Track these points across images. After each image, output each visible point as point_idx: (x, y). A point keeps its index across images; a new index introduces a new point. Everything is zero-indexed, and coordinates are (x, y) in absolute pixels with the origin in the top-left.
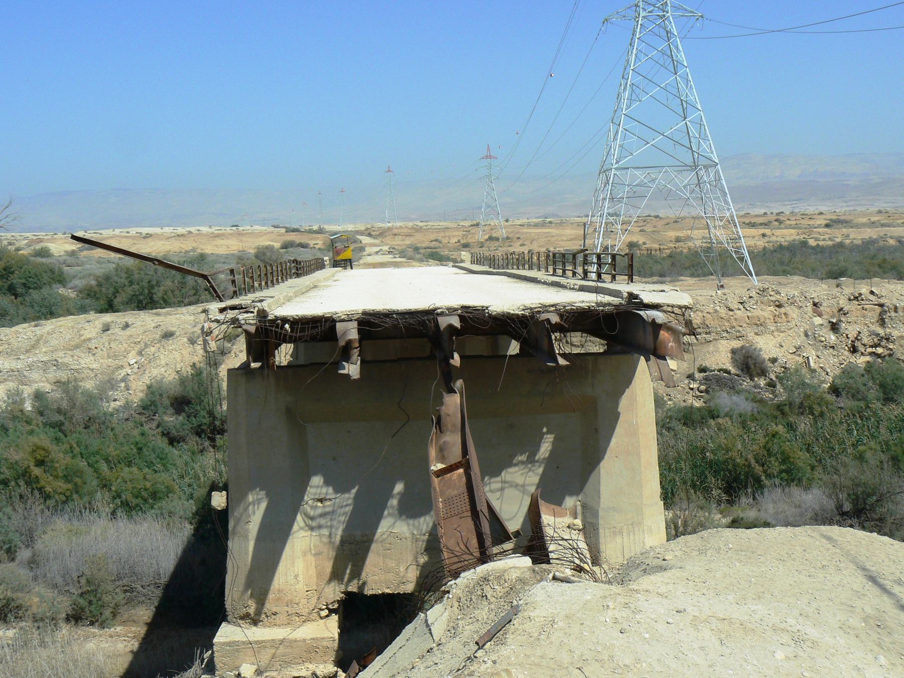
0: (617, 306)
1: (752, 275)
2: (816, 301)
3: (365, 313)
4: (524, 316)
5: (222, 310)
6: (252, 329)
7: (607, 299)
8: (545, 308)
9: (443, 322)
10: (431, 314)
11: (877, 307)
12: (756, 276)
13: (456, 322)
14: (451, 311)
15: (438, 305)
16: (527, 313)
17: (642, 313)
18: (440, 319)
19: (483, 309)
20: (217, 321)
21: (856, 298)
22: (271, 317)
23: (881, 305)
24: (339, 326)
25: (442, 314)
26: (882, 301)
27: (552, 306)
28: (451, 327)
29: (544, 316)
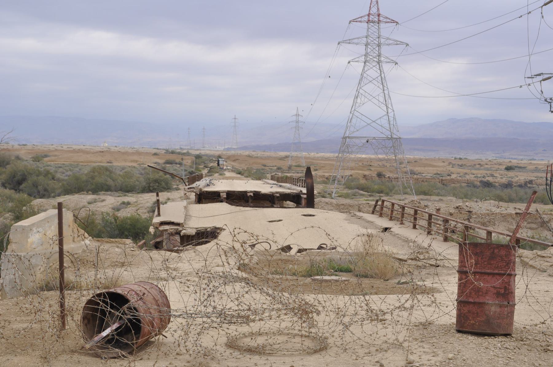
0: (296, 193)
1: (414, 195)
2: (438, 208)
3: (228, 191)
4: (270, 194)
5: (188, 188)
6: (199, 193)
7: (295, 191)
8: (277, 193)
9: (249, 194)
10: (246, 192)
11: (467, 213)
12: (416, 195)
13: (252, 194)
14: (251, 192)
15: (248, 190)
16: (271, 194)
17: (302, 195)
18: (248, 194)
19: (260, 192)
20: (188, 191)
21: (457, 207)
22: (203, 191)
23: (470, 212)
24: (221, 194)
25: (249, 192)
26: (471, 210)
27: (279, 192)
28: (250, 195)
29: (275, 195)
